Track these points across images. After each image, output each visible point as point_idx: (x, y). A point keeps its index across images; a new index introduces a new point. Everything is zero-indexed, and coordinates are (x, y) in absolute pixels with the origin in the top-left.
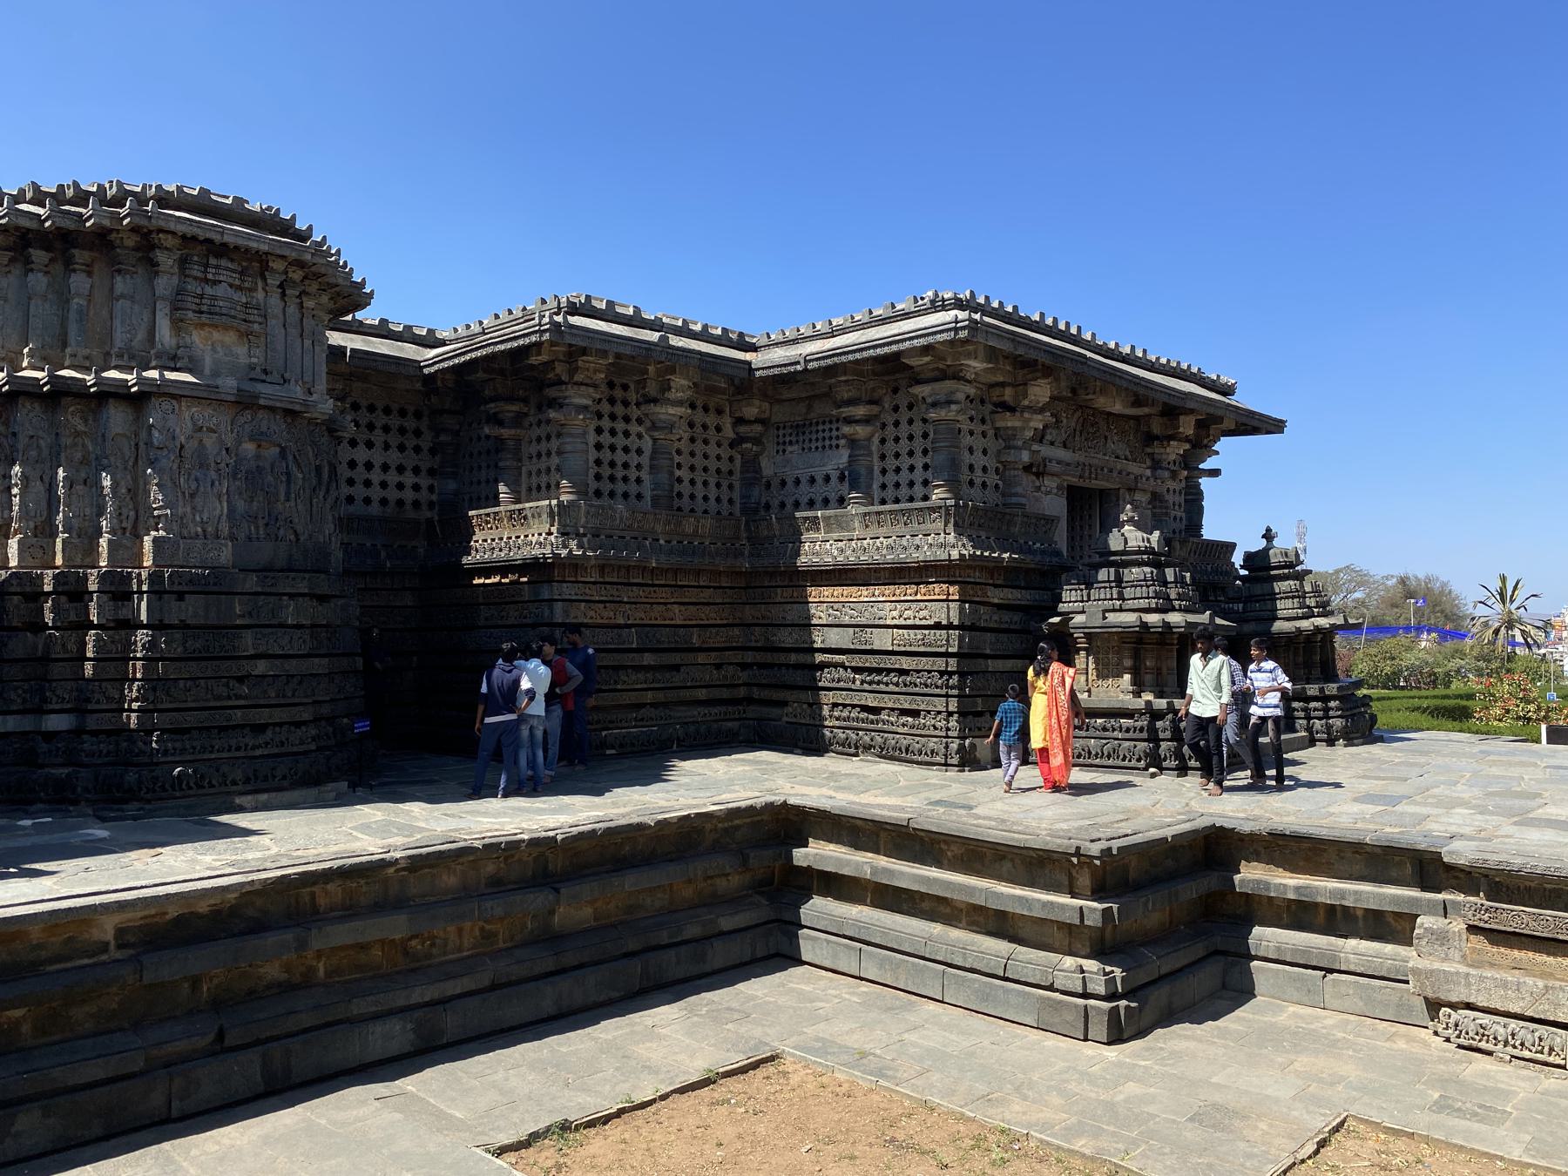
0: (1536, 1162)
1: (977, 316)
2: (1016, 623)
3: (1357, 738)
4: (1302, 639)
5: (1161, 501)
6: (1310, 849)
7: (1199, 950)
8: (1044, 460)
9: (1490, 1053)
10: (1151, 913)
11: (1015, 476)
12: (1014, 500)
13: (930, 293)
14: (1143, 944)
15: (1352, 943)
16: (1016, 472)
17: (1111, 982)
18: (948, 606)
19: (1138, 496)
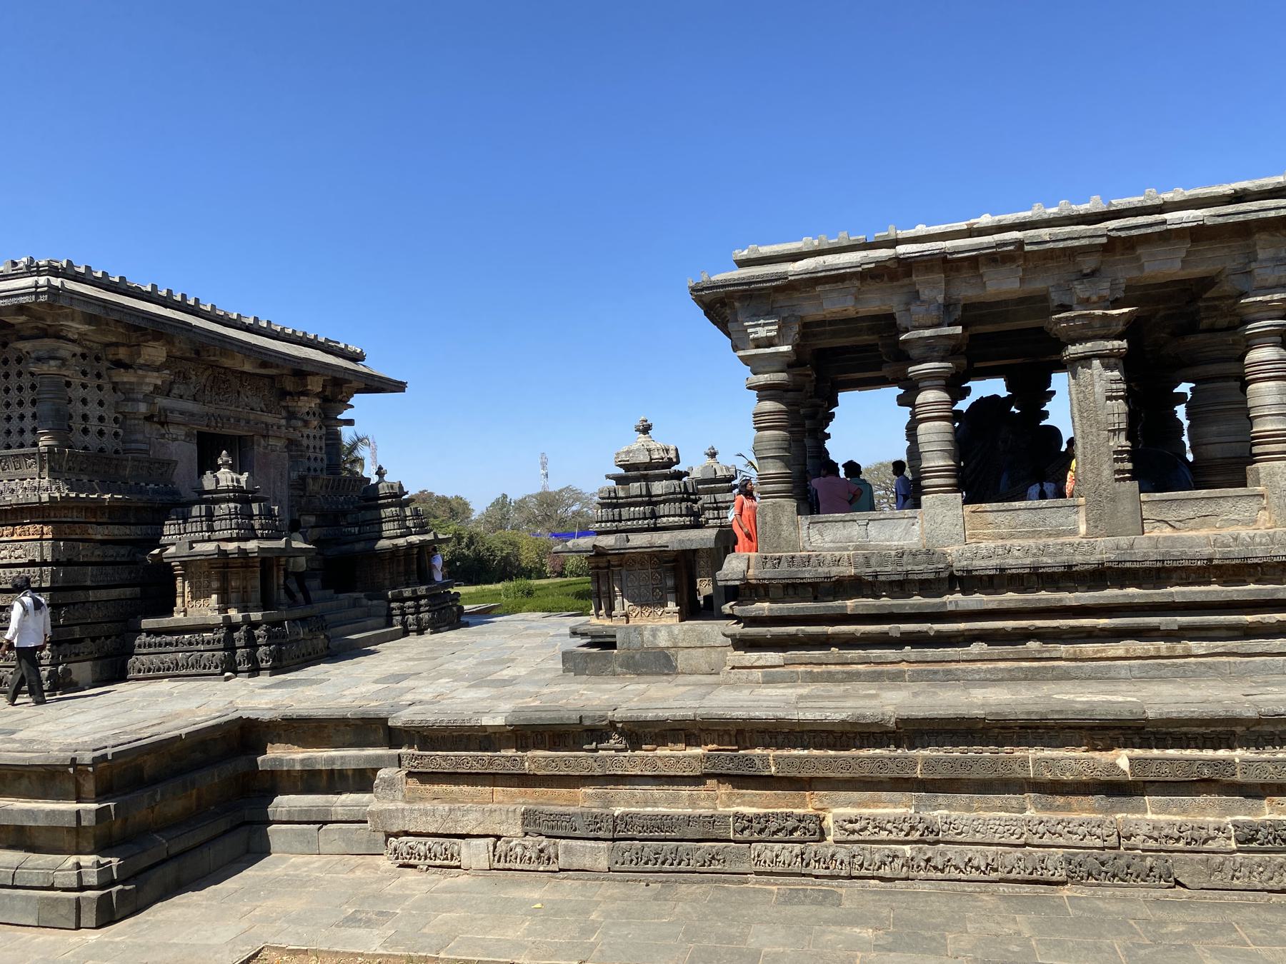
0: (385, 952)
1: (56, 282)
2: (123, 555)
3: (445, 626)
4: (401, 553)
5: (297, 446)
6: (316, 727)
7: (222, 824)
8: (165, 410)
9: (414, 867)
10: (173, 802)
11: (135, 425)
12: (133, 446)
13: (25, 259)
14: (157, 831)
15: (344, 797)
16: (136, 422)
17: (103, 870)
18: (41, 545)
19: (272, 442)
